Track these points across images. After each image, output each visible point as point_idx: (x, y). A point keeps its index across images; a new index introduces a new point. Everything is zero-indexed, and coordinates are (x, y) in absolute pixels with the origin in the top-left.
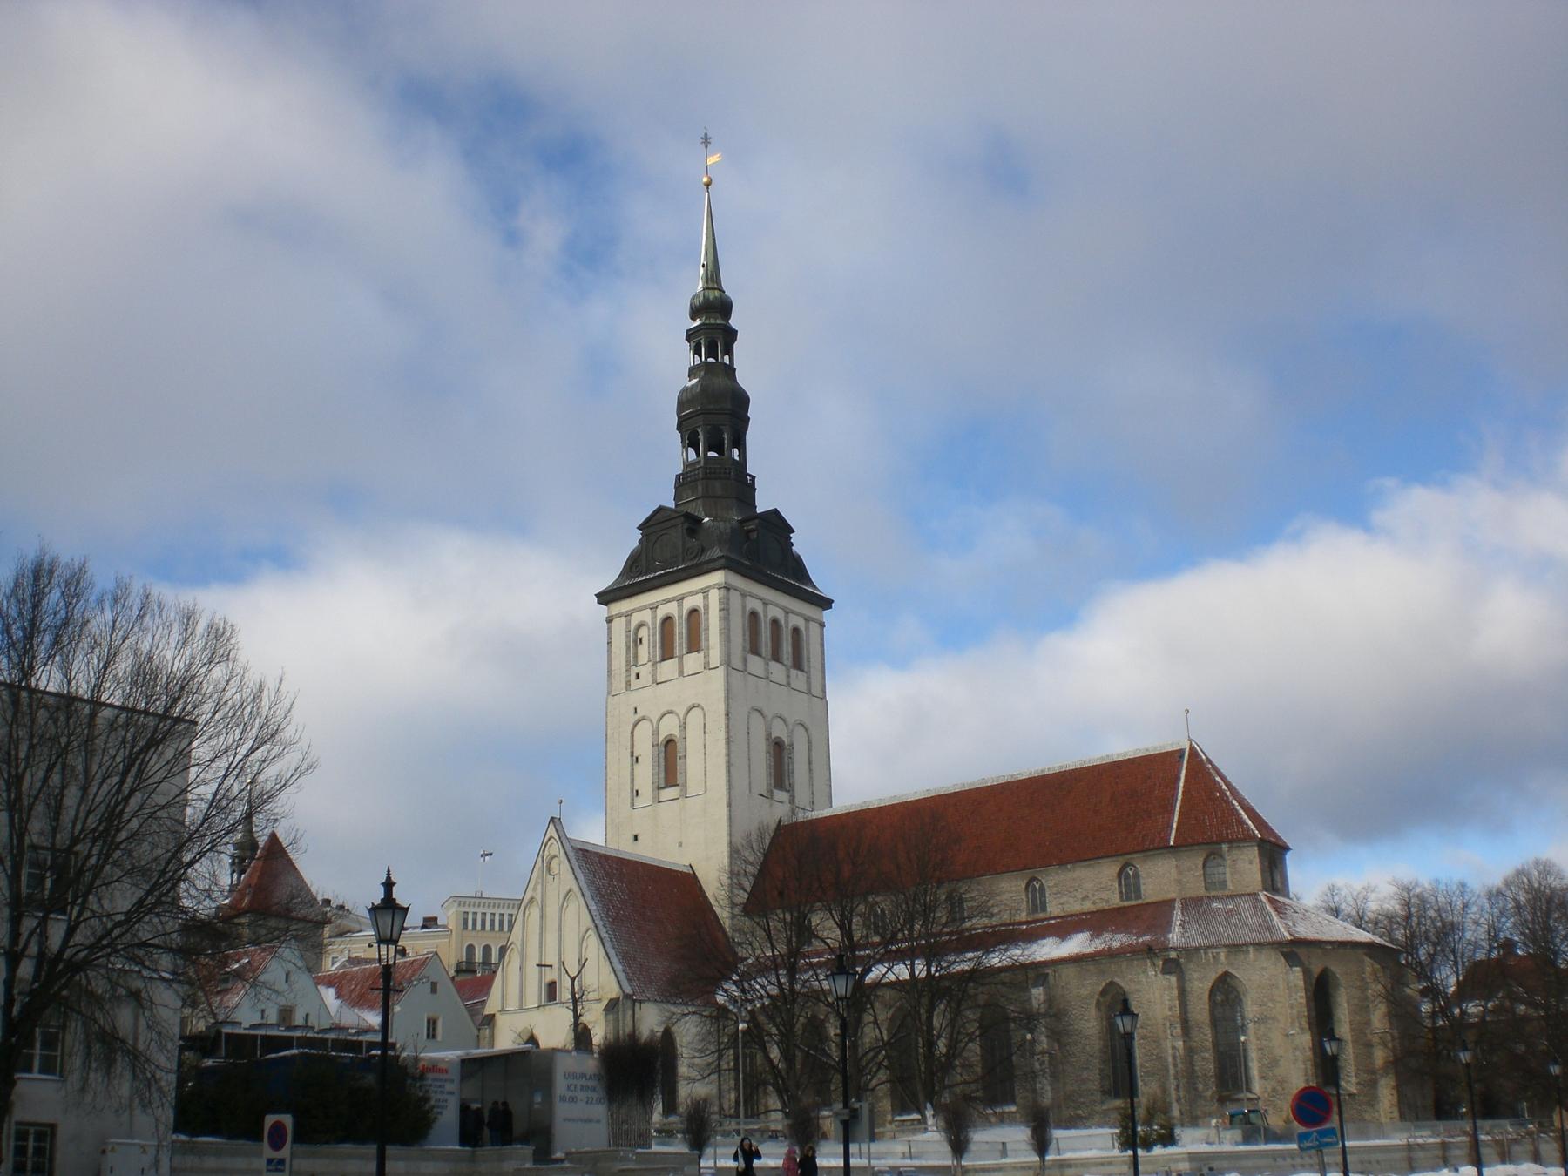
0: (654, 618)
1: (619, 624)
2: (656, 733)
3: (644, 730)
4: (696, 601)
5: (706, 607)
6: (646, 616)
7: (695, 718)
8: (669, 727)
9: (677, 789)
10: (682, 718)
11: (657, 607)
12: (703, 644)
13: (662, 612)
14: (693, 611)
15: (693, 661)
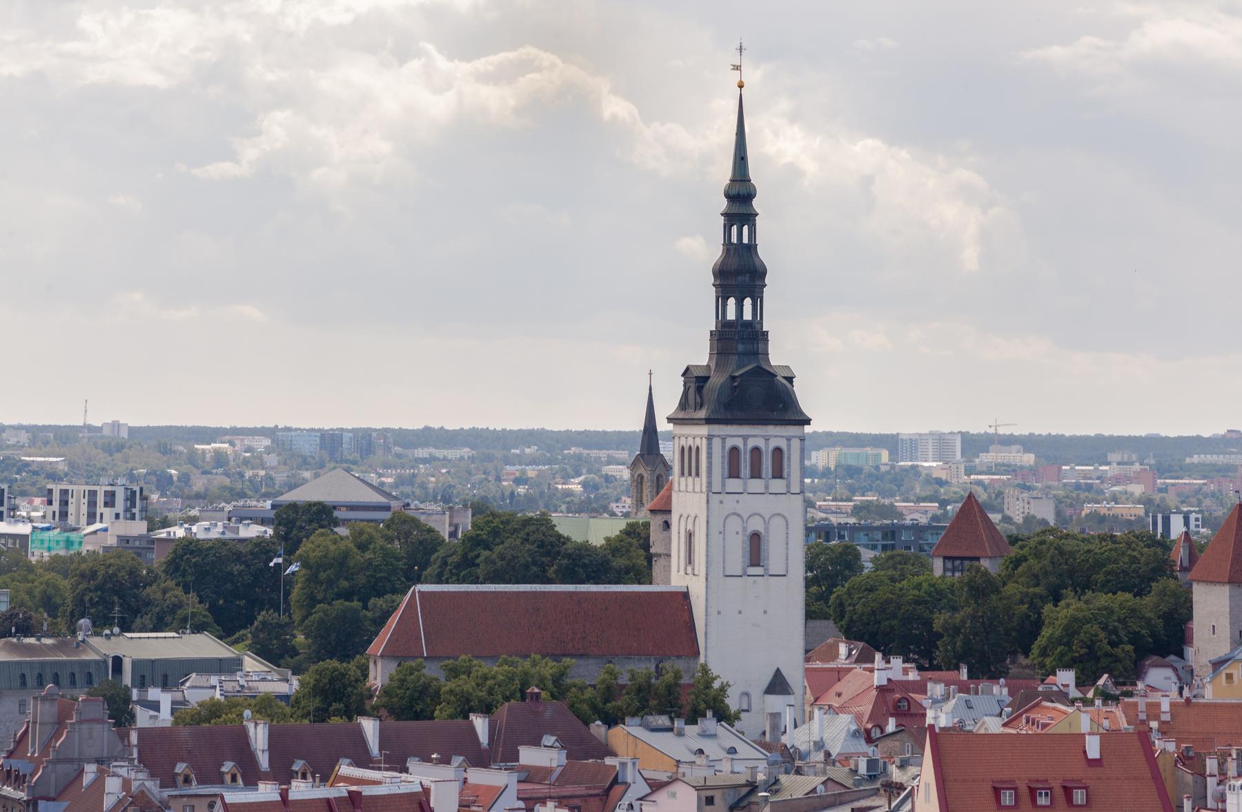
0: (745, 444)
1: (717, 443)
2: (744, 529)
3: (734, 524)
4: (782, 444)
5: (789, 449)
6: (739, 443)
7: (777, 523)
8: (756, 525)
9: (762, 568)
10: (767, 520)
11: (747, 439)
12: (785, 474)
13: (752, 443)
14: (778, 451)
15: (778, 485)
